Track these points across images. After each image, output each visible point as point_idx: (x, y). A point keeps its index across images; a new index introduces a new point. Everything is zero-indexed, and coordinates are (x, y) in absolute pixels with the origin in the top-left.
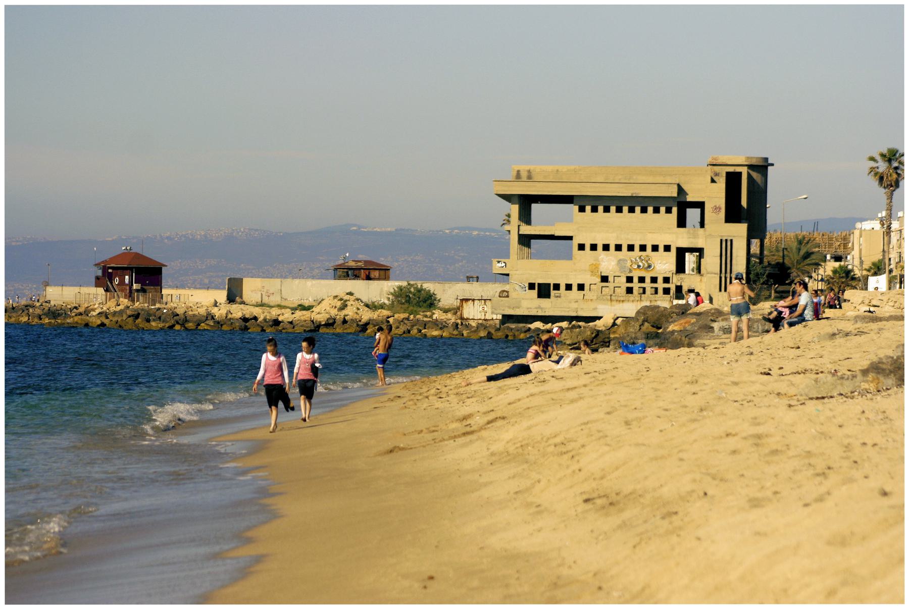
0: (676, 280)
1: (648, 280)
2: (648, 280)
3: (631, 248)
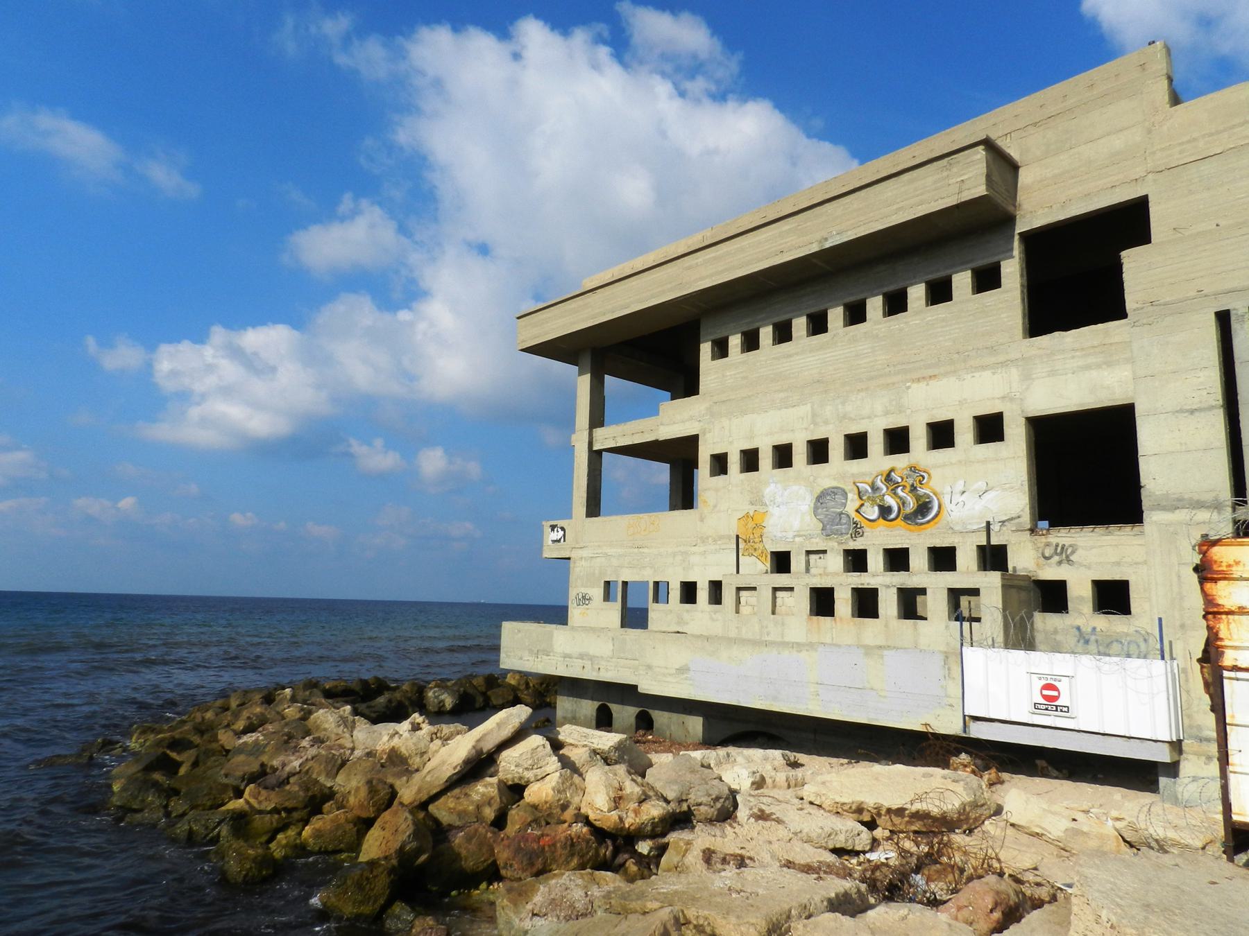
0: (1026, 558)
1: (919, 560)
2: (919, 560)
3: (857, 446)
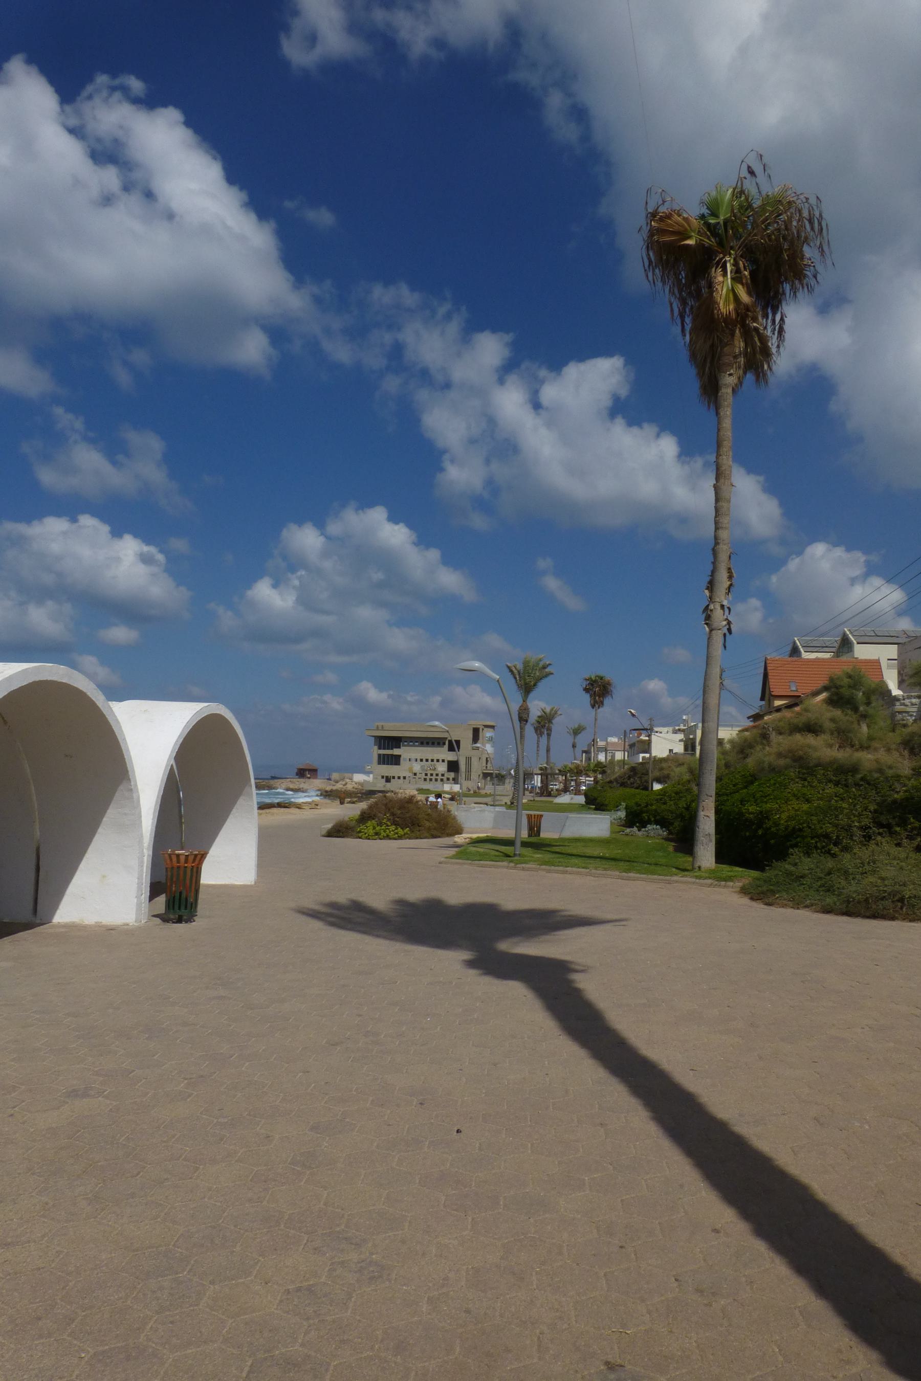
3: (427, 760)
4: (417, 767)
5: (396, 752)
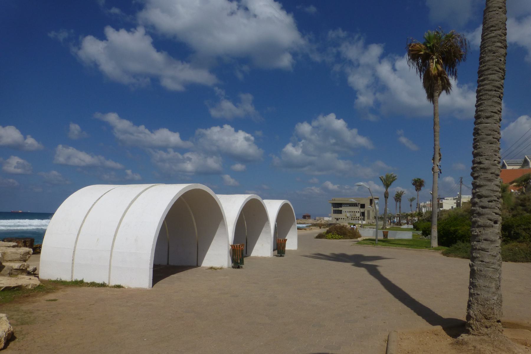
4: (348, 215)
5: (340, 209)
